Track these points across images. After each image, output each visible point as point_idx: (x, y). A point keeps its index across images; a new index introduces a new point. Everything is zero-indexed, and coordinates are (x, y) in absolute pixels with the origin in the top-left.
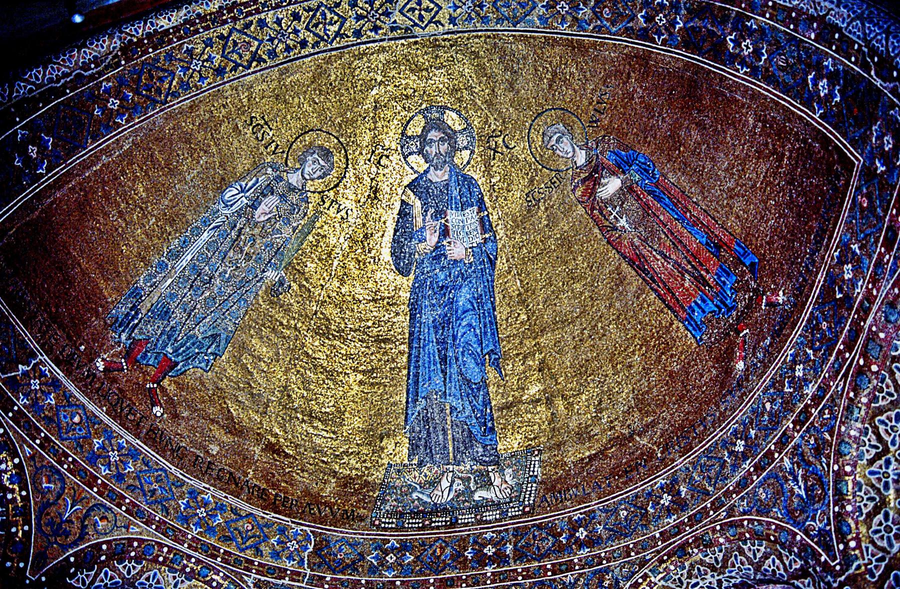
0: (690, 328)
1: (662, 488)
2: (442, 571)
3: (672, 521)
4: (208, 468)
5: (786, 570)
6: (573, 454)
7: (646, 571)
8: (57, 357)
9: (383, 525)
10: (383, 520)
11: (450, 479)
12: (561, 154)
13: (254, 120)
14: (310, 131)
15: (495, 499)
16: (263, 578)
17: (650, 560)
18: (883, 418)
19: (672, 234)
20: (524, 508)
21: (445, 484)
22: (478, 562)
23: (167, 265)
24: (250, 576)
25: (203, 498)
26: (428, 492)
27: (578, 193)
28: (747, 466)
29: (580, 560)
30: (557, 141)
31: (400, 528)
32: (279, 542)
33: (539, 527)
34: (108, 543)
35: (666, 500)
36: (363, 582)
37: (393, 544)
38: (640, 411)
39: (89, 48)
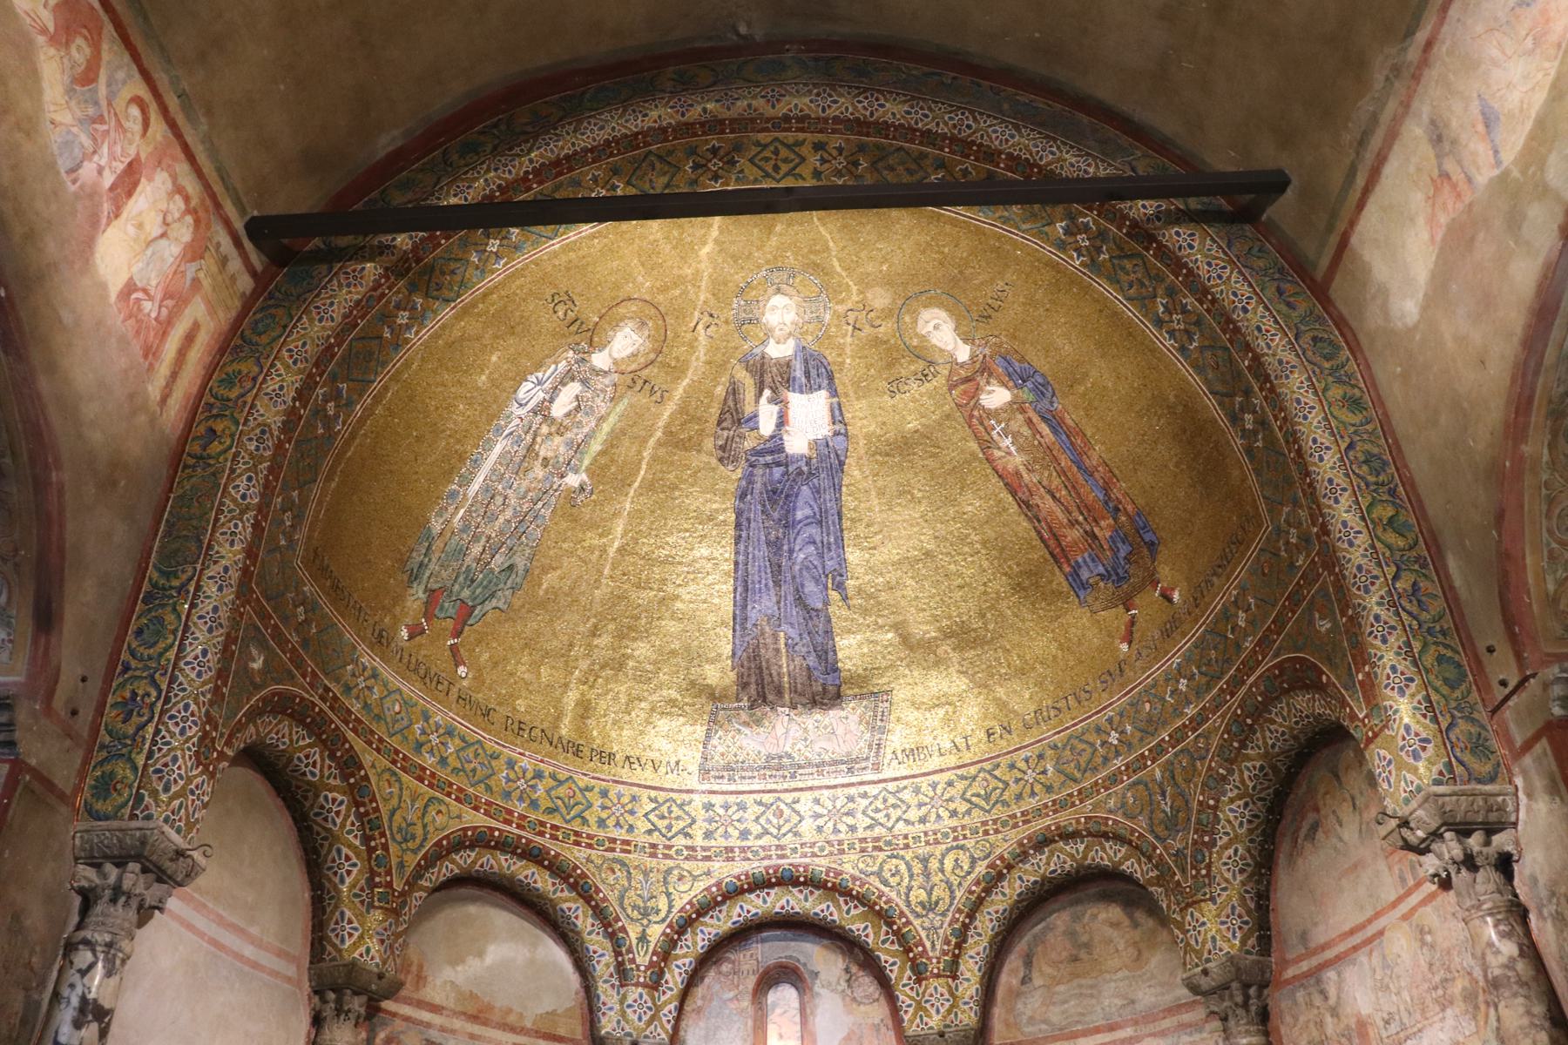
4: (520, 729)
5: (1142, 875)
12: (938, 344)
13: (556, 297)
18: (1249, 765)
19: (1066, 475)
28: (1118, 763)
30: (936, 327)
34: (447, 837)
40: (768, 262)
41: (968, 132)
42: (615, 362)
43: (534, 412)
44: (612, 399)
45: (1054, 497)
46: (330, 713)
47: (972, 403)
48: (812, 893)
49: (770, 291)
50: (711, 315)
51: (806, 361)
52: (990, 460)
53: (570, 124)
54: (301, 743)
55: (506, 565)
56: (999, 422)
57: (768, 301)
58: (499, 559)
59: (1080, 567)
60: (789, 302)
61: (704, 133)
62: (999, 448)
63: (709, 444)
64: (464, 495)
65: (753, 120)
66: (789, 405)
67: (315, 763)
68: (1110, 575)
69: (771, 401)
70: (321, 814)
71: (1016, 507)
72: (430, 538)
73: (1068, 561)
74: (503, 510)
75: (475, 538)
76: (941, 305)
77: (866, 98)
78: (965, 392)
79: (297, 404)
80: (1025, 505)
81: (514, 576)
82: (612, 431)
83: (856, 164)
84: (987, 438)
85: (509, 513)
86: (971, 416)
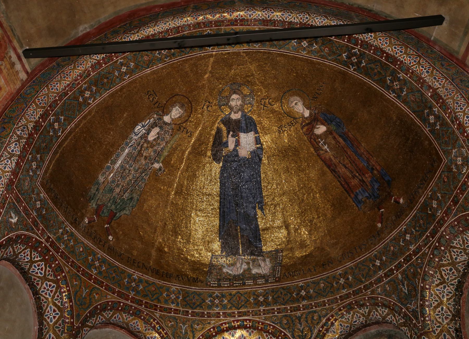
0: (356, 202)
1: (340, 275)
2: (241, 307)
3: (345, 292)
4: (134, 262)
6: (298, 254)
7: (334, 313)
8: (71, 222)
9: (212, 285)
10: (212, 282)
11: (241, 263)
12: (297, 111)
14: (175, 96)
15: (262, 273)
16: (163, 313)
17: (335, 308)
19: (350, 158)
20: (276, 278)
21: (238, 265)
22: (256, 304)
23: (110, 167)
24: (157, 313)
25: (133, 277)
26: (231, 268)
27: (304, 130)
29: (303, 306)
30: (296, 104)
31: (219, 286)
32: (167, 295)
33: (283, 288)
34: (100, 304)
35: (342, 281)
36: (206, 313)
37: (217, 294)
38: (330, 237)
39: (77, 69)
40: (230, 81)
41: (307, 20)
42: (172, 120)
43: (141, 138)
44: (171, 135)
45: (346, 167)
46: (50, 248)
47: (311, 133)
48: (252, 332)
49: (232, 93)
50: (209, 102)
51: (245, 120)
52: (319, 155)
53: (153, 23)
54: (36, 259)
55: (130, 197)
56: (322, 140)
57: (231, 97)
58: (127, 195)
59: (358, 194)
60: (239, 97)
61: (204, 27)
62: (322, 150)
63: (209, 153)
64: (113, 168)
65: (223, 21)
66: (240, 138)
67: (42, 268)
69: (233, 136)
70: (44, 291)
71: (330, 172)
72: (98, 184)
73: (353, 192)
74: (128, 176)
75: (118, 186)
76: (299, 95)
77: (266, 10)
78: (308, 129)
79: (41, 120)
80: (333, 171)
81: (133, 202)
82: (172, 147)
84: (317, 146)
85: (131, 177)
86: (311, 138)
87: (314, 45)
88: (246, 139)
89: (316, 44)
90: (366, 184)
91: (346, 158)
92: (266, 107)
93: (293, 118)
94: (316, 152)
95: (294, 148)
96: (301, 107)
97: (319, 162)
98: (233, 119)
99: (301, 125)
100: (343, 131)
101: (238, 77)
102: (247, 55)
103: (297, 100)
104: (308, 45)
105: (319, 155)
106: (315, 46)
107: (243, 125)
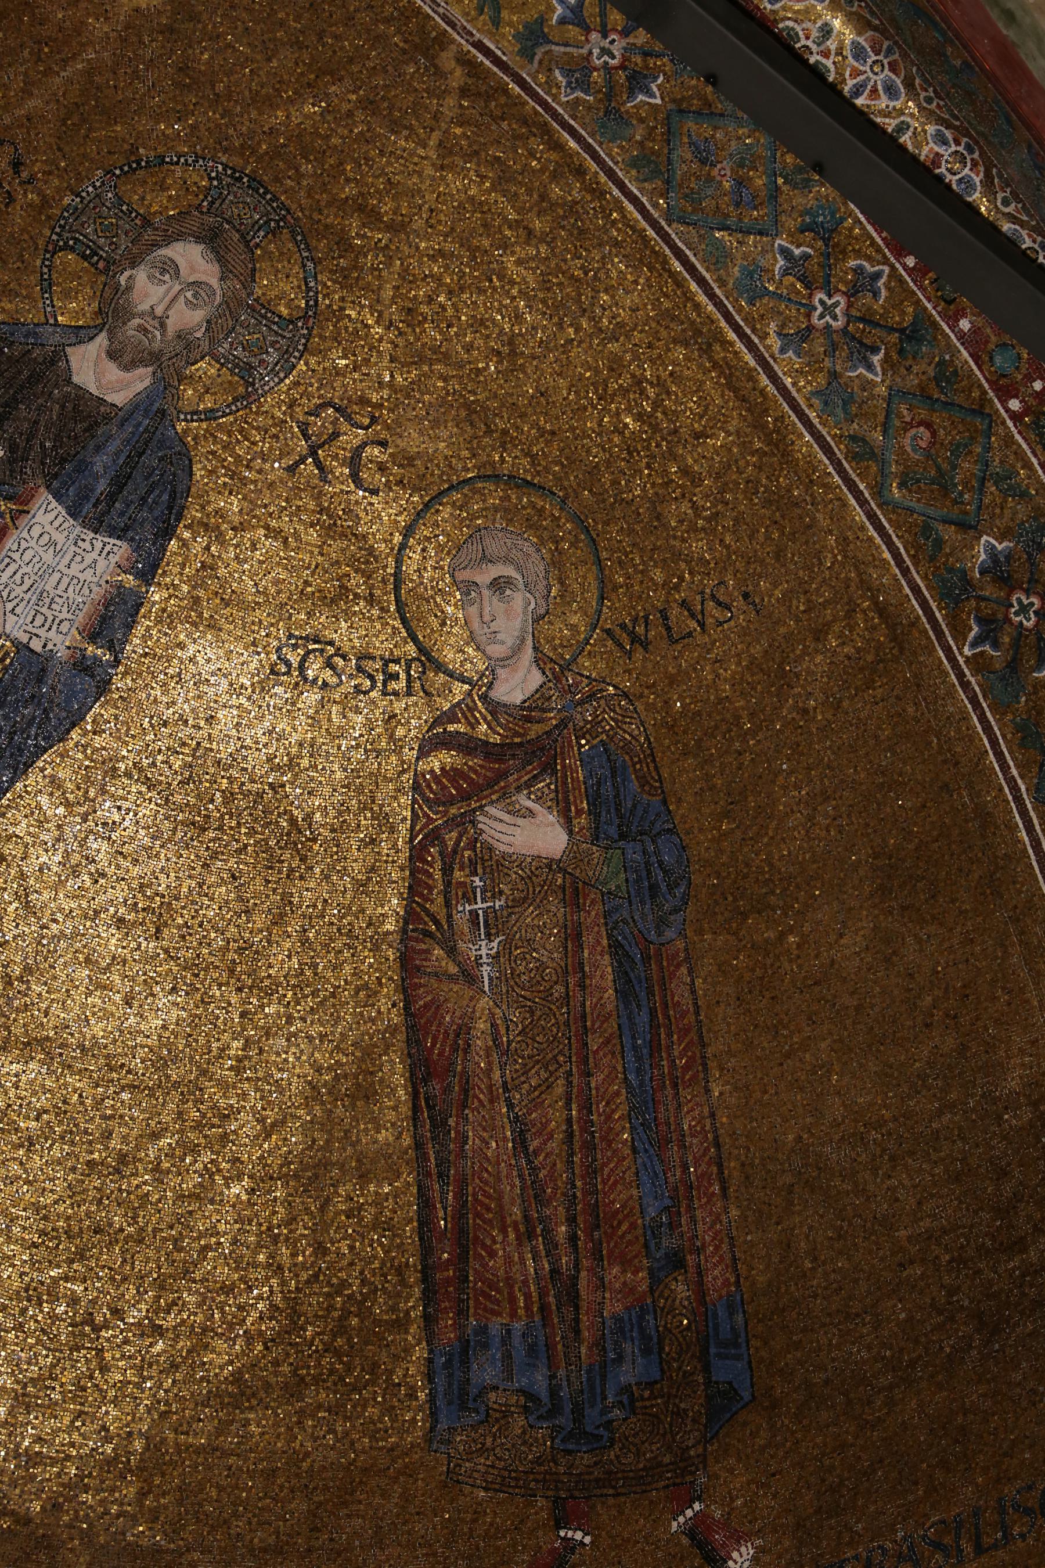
19: (587, 1107)
27: (435, 763)
30: (498, 585)
45: (521, 1141)
57: (169, 240)
60: (214, 282)
62: (452, 952)
68: (555, 1410)
71: (405, 1110)
73: (462, 1313)
78: (451, 774)
83: (637, 81)
87: (876, 359)
88: (48, 557)
89: (886, 360)
90: (577, 1320)
91: (559, 1089)
92: (318, 464)
93: (421, 649)
94: (404, 931)
95: (293, 821)
96: (517, 623)
97: (384, 1004)
98: (75, 379)
99: (437, 722)
100: (653, 936)
101: (307, 168)
102: (464, 92)
103: (518, 568)
104: (844, 331)
105: (408, 963)
106: (870, 367)
107: (100, 462)
